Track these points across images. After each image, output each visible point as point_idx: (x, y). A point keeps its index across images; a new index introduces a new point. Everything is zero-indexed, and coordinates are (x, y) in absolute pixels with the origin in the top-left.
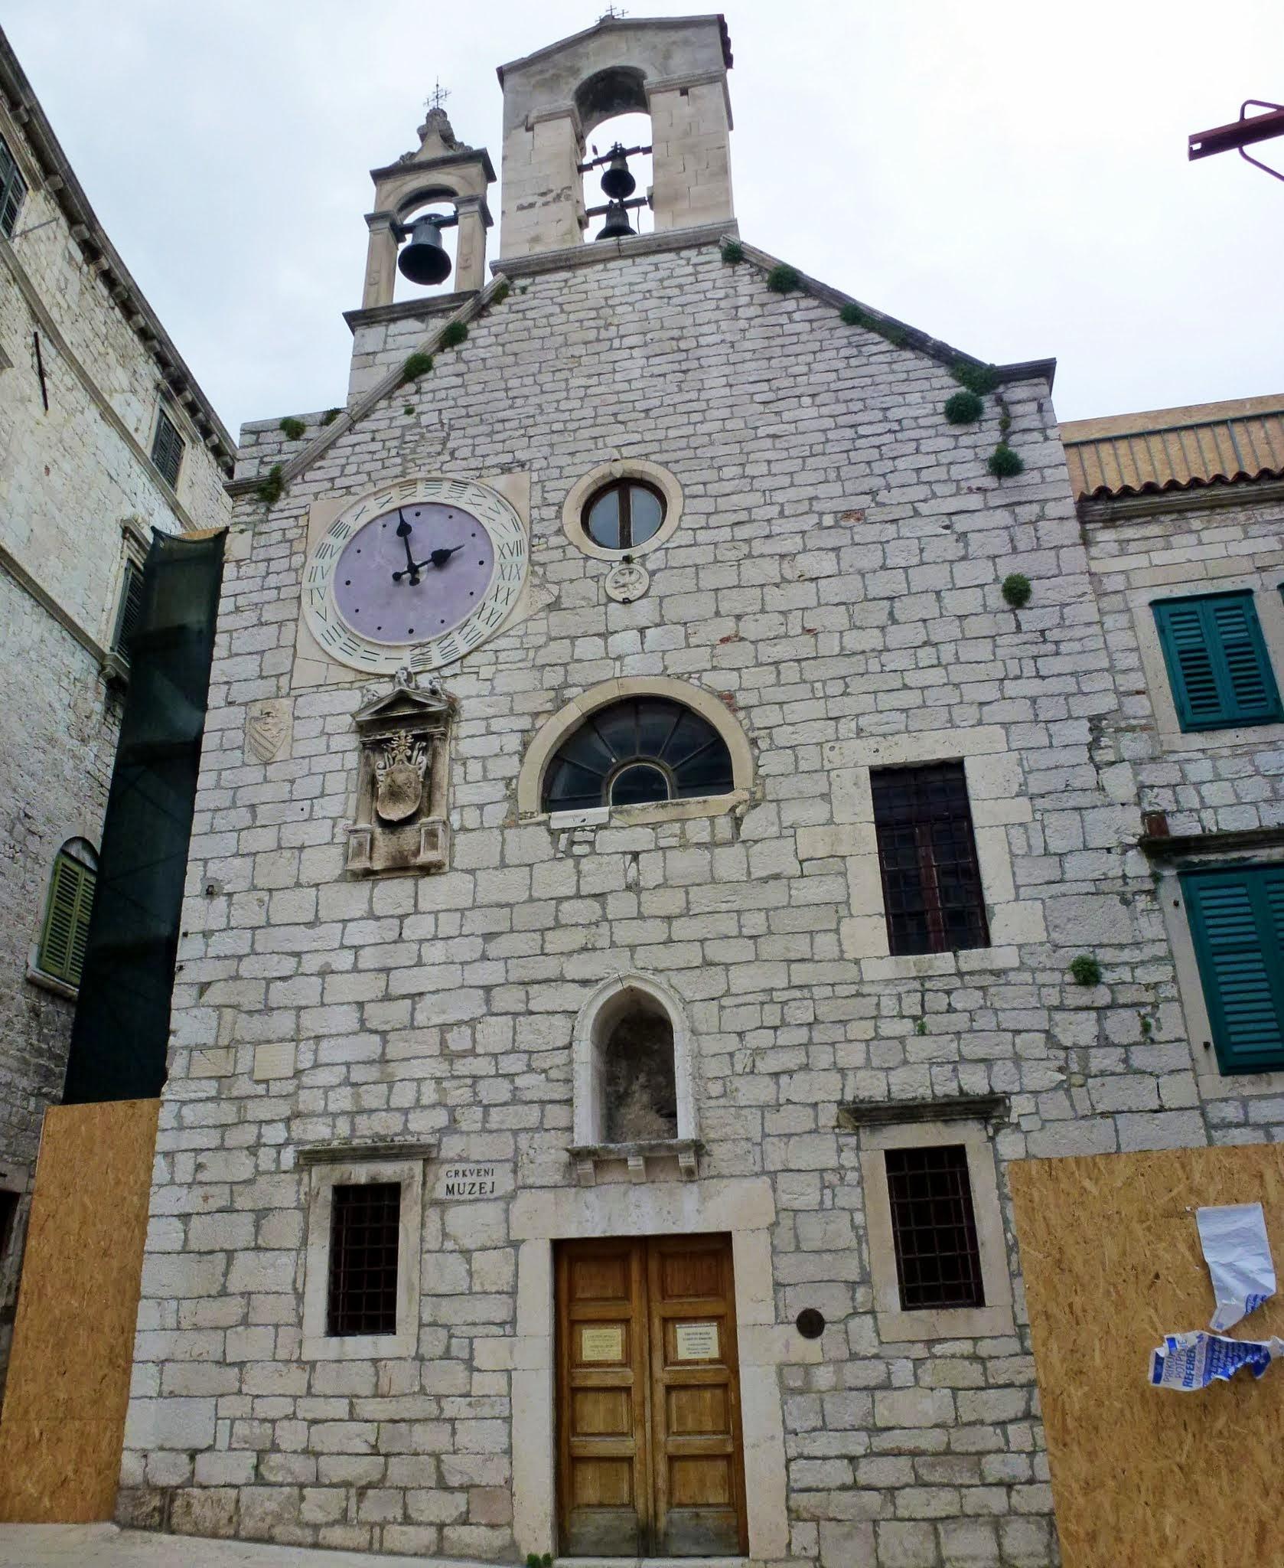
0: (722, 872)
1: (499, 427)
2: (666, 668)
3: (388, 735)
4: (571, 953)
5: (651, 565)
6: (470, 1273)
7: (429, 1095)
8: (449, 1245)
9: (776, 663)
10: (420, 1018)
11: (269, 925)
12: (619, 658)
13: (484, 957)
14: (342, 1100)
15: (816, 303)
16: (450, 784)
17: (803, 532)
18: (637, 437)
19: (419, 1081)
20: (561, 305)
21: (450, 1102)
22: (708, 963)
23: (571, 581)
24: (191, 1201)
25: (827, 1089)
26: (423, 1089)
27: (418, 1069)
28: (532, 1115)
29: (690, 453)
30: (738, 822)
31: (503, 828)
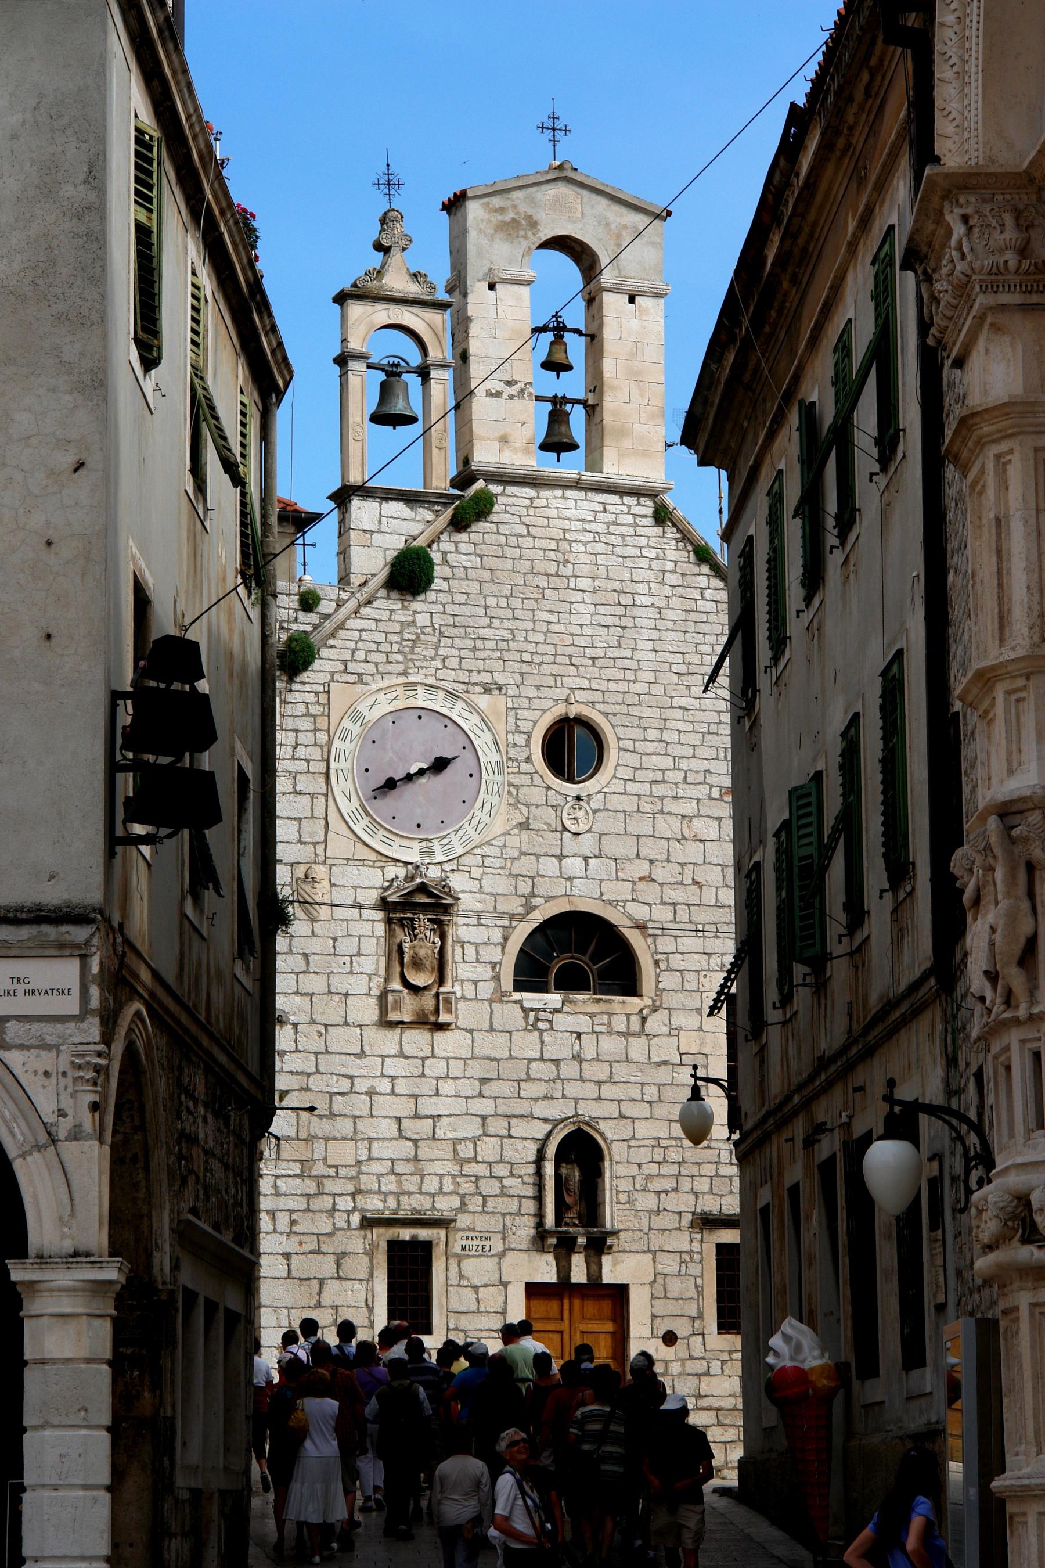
0: (634, 1055)
1: (480, 644)
2: (602, 894)
3: (409, 915)
4: (536, 1100)
5: (594, 805)
6: (478, 1300)
7: (448, 1185)
8: (465, 1282)
9: (674, 904)
10: (439, 1133)
11: (327, 1052)
12: (569, 879)
13: (481, 1095)
14: (389, 1184)
15: (721, 585)
16: (454, 962)
17: (698, 800)
18: (585, 684)
19: (441, 1176)
20: (528, 526)
21: (461, 1192)
22: (622, 1116)
23: (537, 806)
24: (290, 1245)
25: (685, 1204)
26: (444, 1182)
27: (439, 1168)
28: (513, 1205)
29: (624, 709)
30: (644, 1020)
31: (491, 1001)
